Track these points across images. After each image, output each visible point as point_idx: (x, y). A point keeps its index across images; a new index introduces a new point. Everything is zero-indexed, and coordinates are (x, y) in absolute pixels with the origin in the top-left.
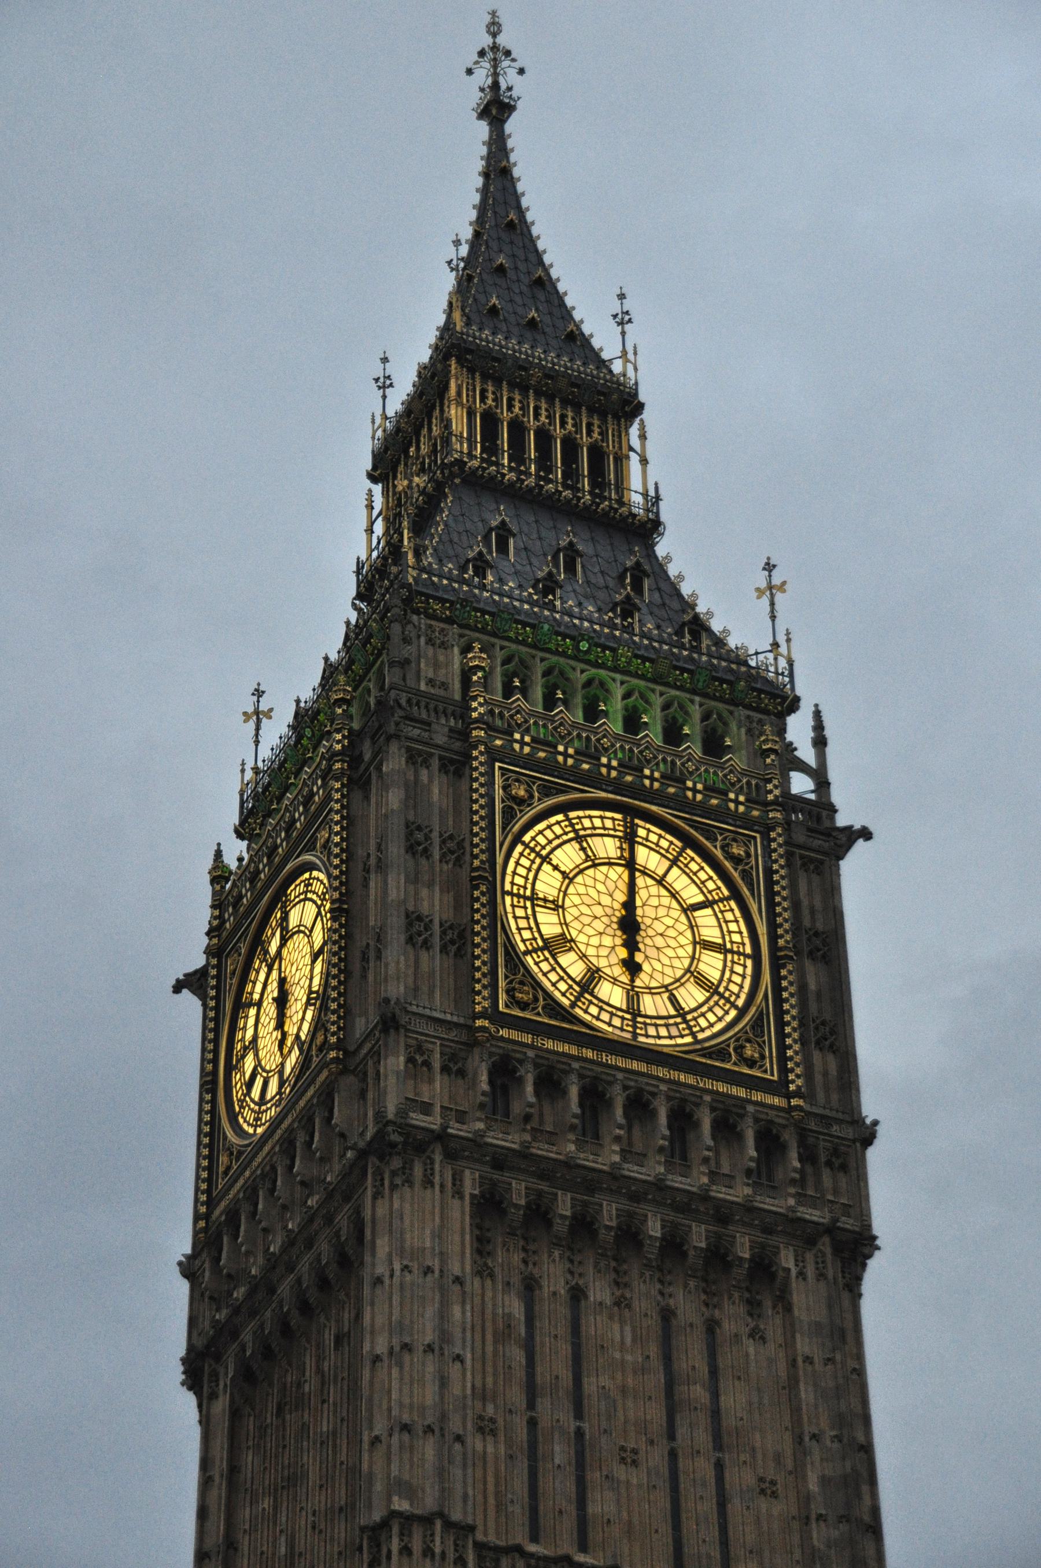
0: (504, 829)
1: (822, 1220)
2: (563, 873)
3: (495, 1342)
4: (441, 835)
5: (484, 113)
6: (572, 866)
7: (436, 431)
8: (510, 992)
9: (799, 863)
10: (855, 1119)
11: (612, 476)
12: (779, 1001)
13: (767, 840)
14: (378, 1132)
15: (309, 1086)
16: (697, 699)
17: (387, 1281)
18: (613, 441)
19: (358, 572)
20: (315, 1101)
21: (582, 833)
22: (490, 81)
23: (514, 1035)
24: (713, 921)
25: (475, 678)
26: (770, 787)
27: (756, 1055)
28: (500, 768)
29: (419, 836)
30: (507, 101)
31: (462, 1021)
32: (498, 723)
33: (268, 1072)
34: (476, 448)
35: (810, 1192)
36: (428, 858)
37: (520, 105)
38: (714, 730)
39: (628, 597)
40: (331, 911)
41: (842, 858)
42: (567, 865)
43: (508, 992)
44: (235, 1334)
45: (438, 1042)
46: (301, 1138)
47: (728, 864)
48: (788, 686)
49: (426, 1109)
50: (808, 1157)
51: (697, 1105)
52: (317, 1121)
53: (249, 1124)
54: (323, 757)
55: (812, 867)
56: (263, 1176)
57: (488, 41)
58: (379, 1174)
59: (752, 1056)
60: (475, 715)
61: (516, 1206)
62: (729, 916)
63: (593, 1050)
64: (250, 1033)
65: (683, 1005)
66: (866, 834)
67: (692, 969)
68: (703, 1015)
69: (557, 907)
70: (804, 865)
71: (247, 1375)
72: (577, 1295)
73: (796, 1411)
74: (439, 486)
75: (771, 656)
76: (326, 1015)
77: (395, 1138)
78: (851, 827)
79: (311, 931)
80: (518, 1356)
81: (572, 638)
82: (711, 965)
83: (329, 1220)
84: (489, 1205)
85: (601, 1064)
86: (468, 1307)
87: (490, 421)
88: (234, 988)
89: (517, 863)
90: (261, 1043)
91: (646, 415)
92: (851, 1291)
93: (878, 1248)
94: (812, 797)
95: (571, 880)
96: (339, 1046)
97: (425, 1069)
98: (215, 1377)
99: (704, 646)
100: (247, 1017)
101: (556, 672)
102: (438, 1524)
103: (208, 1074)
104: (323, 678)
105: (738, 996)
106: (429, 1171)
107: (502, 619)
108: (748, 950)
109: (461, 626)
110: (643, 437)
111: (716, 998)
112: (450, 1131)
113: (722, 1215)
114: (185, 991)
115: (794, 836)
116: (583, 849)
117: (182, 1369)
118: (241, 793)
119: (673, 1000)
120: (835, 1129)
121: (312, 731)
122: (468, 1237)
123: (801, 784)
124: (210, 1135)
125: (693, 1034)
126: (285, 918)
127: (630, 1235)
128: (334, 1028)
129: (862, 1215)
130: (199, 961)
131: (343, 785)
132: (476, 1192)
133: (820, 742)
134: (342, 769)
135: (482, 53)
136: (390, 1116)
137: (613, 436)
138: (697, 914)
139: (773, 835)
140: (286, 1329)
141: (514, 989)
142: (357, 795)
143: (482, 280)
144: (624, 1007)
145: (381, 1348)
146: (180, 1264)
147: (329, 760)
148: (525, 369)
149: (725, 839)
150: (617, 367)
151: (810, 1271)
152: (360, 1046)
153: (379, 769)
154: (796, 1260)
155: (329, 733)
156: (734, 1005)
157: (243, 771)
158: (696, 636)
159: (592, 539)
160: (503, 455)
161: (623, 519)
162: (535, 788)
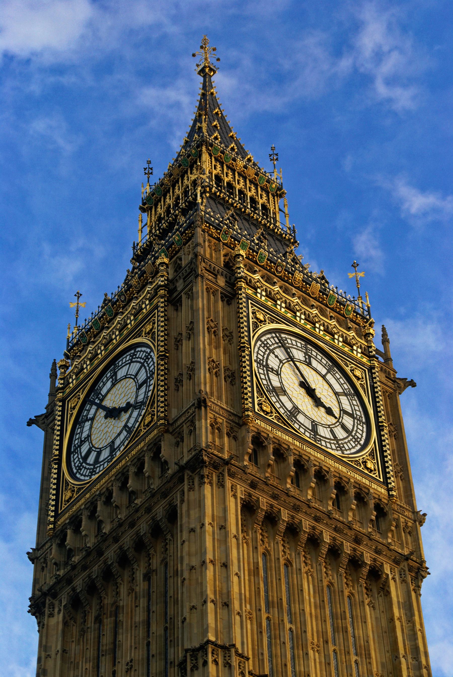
0: (253, 331)
2: (280, 360)
3: (249, 575)
8: (260, 404)
12: (381, 446)
16: (328, 309)
17: (198, 530)
19: (134, 248)
20: (145, 448)
25: (238, 260)
29: (212, 325)
31: (235, 413)
41: (400, 394)
43: (258, 405)
45: (225, 420)
46: (133, 470)
52: (146, 459)
56: (100, 495)
58: (191, 479)
62: (354, 403)
64: (85, 435)
66: (413, 384)
69: (278, 374)
71: (76, 603)
72: (288, 564)
77: (206, 458)
78: (406, 379)
82: (348, 422)
83: (149, 510)
84: (248, 508)
85: (303, 450)
89: (259, 348)
92: (415, 592)
95: (283, 364)
97: (216, 431)
98: (52, 606)
105: (361, 440)
106: (221, 480)
108: (364, 420)
114: (34, 426)
118: (68, 339)
126: (115, 374)
130: (44, 411)
132: (243, 497)
133: (385, 341)
138: (340, 397)
142: (170, 308)
144: (310, 428)
145: (195, 562)
146: (28, 553)
154: (391, 571)
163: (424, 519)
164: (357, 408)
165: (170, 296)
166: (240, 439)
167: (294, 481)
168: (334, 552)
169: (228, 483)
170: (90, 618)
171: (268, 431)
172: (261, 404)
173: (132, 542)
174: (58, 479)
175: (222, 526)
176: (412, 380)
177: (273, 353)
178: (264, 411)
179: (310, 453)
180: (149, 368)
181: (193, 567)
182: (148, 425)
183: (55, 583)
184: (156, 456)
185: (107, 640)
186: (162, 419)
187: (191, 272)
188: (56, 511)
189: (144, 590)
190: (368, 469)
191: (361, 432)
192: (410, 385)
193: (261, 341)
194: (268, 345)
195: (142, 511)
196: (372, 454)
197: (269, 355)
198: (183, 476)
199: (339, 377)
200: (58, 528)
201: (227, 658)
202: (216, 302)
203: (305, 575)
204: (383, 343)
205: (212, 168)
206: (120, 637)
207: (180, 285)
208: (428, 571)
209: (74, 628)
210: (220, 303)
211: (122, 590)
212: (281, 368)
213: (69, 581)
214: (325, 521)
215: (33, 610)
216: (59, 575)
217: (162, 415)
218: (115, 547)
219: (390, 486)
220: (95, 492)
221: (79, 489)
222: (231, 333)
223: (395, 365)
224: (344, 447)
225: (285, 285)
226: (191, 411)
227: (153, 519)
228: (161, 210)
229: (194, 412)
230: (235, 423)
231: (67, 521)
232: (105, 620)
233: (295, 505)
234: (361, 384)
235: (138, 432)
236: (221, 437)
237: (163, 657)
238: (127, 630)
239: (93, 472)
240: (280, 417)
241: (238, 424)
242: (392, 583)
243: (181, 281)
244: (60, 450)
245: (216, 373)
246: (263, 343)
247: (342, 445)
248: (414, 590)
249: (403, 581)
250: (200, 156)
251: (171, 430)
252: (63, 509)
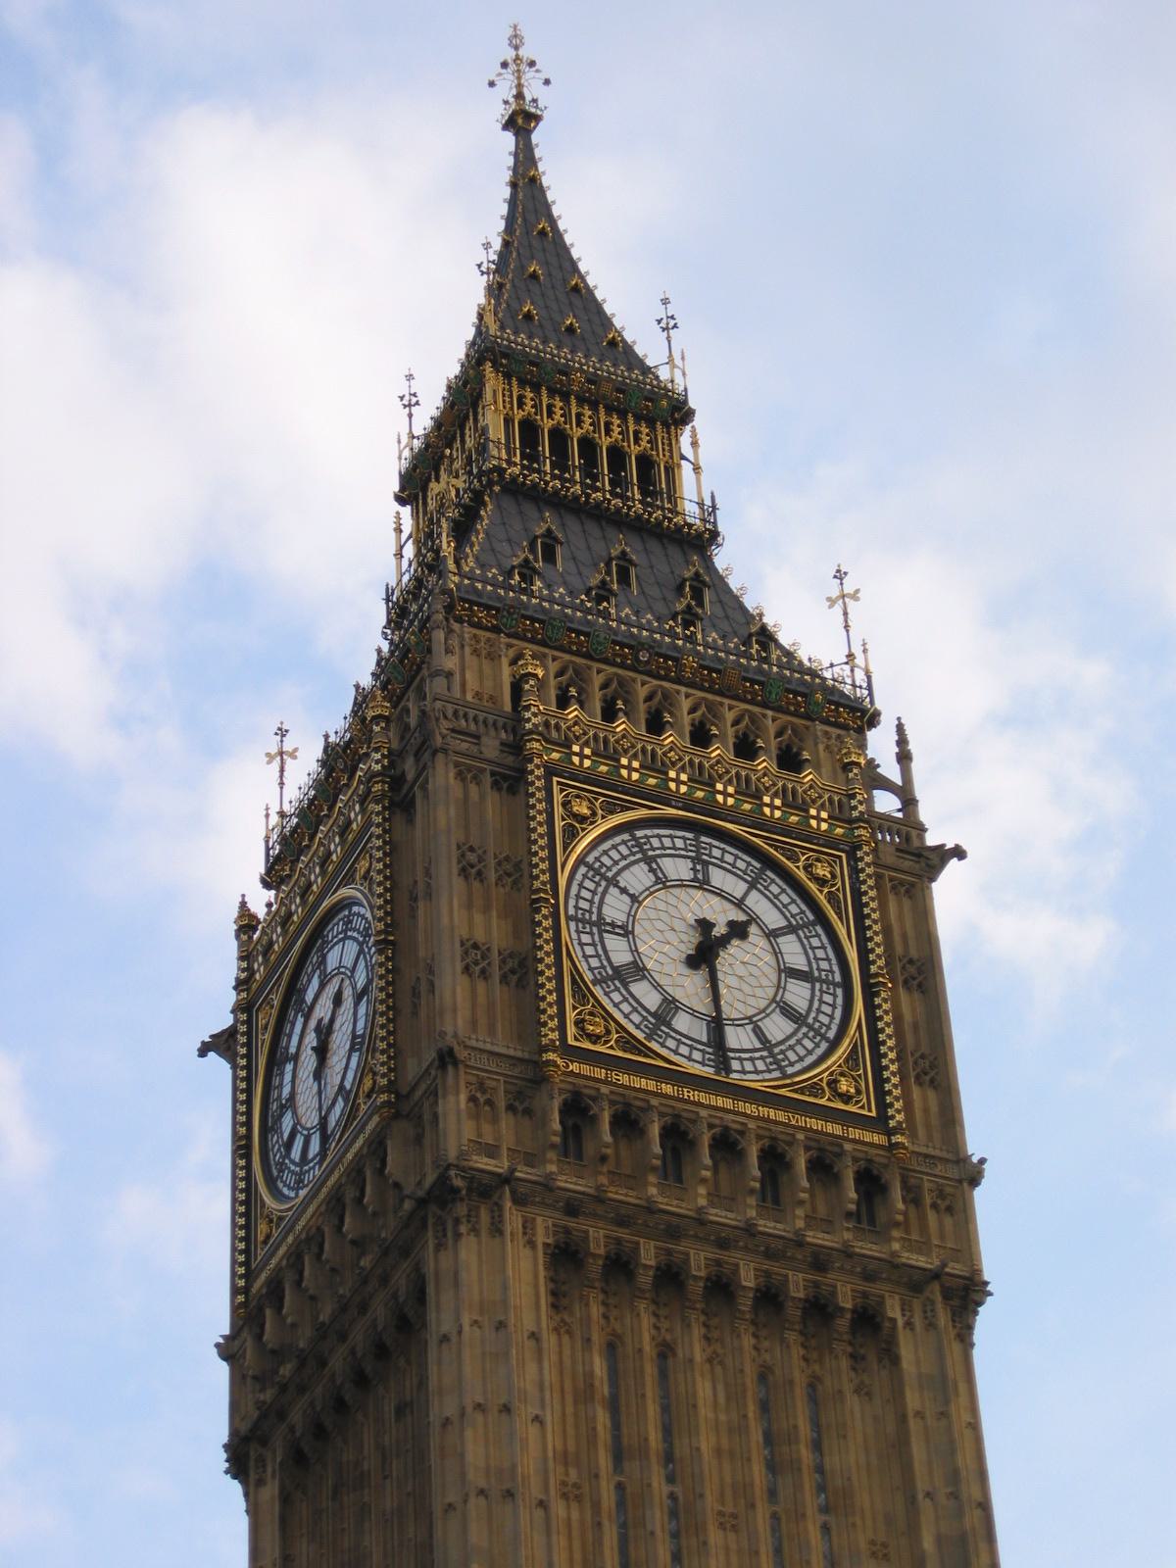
0: (565, 849)
1: (929, 1266)
2: (634, 898)
3: (576, 1402)
4: (496, 857)
5: (510, 124)
6: (641, 888)
7: (470, 443)
9: (889, 885)
10: (960, 1159)
11: (664, 486)
12: (874, 1032)
13: (853, 858)
14: (439, 1178)
15: (356, 1137)
16: (770, 713)
17: (454, 1339)
18: (663, 450)
19: (388, 600)
20: (365, 1151)
21: (650, 853)
22: (514, 92)
23: (586, 1070)
24: (798, 948)
25: (527, 687)
26: (853, 803)
27: (852, 1090)
28: (559, 783)
29: (472, 857)
30: (533, 110)
31: (526, 1056)
32: (554, 734)
33: (308, 1129)
34: (515, 455)
35: (914, 1236)
36: (482, 881)
37: (545, 115)
38: (789, 747)
39: (689, 606)
40: (377, 943)
41: (933, 879)
42: (635, 888)
44: (282, 1415)
46: (350, 1194)
47: (813, 887)
48: (868, 700)
49: (492, 1151)
50: (913, 1197)
51: (790, 1144)
52: (368, 1174)
53: (289, 1188)
54: (360, 782)
55: (903, 890)
56: (308, 1240)
57: (510, 54)
58: (441, 1223)
59: (848, 1091)
60: (528, 726)
61: (594, 1256)
62: (815, 942)
63: (673, 1086)
64: (286, 1091)
65: (770, 1037)
66: (959, 853)
67: (778, 999)
68: (791, 1048)
69: (626, 931)
70: (894, 888)
71: (298, 1458)
74: (478, 498)
75: (847, 668)
76: (373, 1058)
77: (458, 1182)
78: (943, 845)
79: (353, 970)
80: (602, 1418)
81: (630, 647)
82: (798, 994)
83: (385, 1280)
84: (565, 1256)
85: (683, 1100)
86: (546, 1365)
87: (529, 429)
88: (267, 1044)
89: (581, 886)
90: (300, 1100)
91: (698, 421)
93: (990, 1294)
94: (900, 815)
95: (640, 903)
96: (391, 1087)
97: (487, 1108)
98: (261, 1461)
99: (774, 656)
100: (282, 1074)
101: (614, 685)
103: (241, 1138)
104: (355, 704)
105: (829, 1027)
107: (554, 627)
108: (838, 978)
109: (508, 635)
110: (695, 444)
111: (804, 1030)
112: (518, 1174)
113: (819, 1262)
114: (212, 1054)
115: (881, 855)
116: (651, 870)
118: (267, 842)
119: (758, 1032)
120: (939, 1169)
121: (345, 763)
122: (542, 1289)
123: (886, 803)
124: (247, 1203)
125: (781, 1068)
126: (323, 961)
127: (721, 1287)
128: (384, 1069)
129: (972, 1260)
130: (227, 1021)
131: (384, 808)
132: (549, 1241)
133: (904, 757)
134: (383, 790)
135: (504, 65)
137: (663, 444)
138: (778, 940)
139: (859, 854)
140: (340, 1406)
141: (583, 1021)
143: (514, 286)
145: (450, 1410)
146: (217, 1345)
147: (369, 781)
148: (566, 374)
149: (807, 859)
150: (664, 374)
152: (413, 1089)
153: (424, 788)
154: (903, 1310)
155: (367, 755)
156: (824, 1037)
157: (267, 816)
158: (764, 647)
159: (646, 549)
160: (545, 461)
161: (679, 529)
162: (597, 804)
168: (770, 1298)
169: (513, 1219)
175: (500, 1323)
180: (371, 958)
183: (259, 1419)
186: (383, 1093)
193: (587, 865)
194: (603, 870)
196: (853, 1056)
202: (482, 797)
205: (512, 409)
207: (409, 767)
208: (989, 1288)
212: (634, 917)
214: (741, 1244)
216: (264, 1402)
220: (301, 1233)
221: (281, 1219)
223: (924, 814)
224: (787, 1058)
225: (661, 686)
231: (264, 1291)
235: (355, 1108)
239: (299, 1184)
245: (483, 971)
247: (780, 1057)
252: (259, 1258)
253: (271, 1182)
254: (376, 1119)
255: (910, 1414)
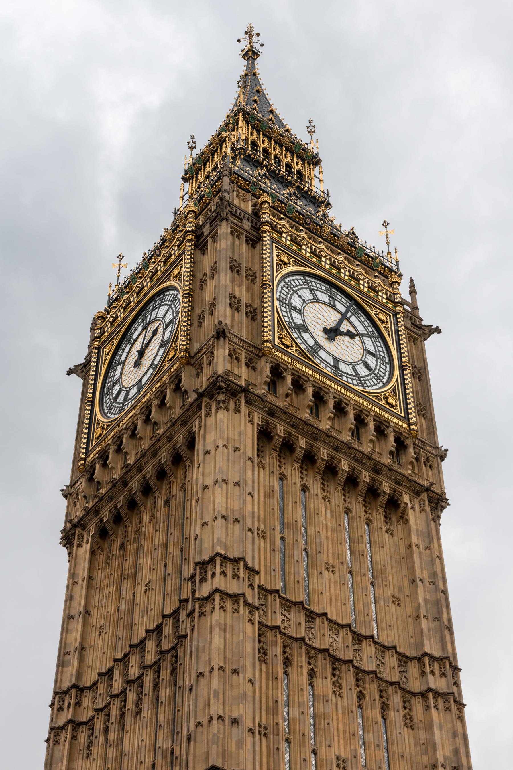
0: (277, 272)
12: (404, 384)
19: (175, 213)
25: (265, 206)
29: (236, 264)
41: (425, 339)
43: (279, 338)
46: (156, 402)
47: (379, 323)
56: (126, 429)
62: (378, 344)
64: (116, 377)
66: (438, 330)
69: (300, 312)
71: (103, 533)
73: (412, 569)
77: (222, 384)
78: (432, 326)
82: (371, 361)
83: (170, 439)
84: (265, 435)
85: (323, 382)
89: (282, 288)
91: (322, 164)
97: (236, 361)
102: (242, 563)
106: (238, 406)
108: (387, 360)
114: (73, 375)
116: (311, 293)
117: (61, 536)
118: (109, 296)
132: (260, 423)
133: (413, 292)
136: (220, 372)
146: (62, 490)
151: (417, 506)
157: (110, 287)
163: (446, 454)
164: (380, 349)
165: (197, 241)
166: (259, 370)
167: (314, 411)
170: (115, 545)
171: (288, 363)
172: (282, 338)
173: (154, 471)
174: (90, 419)
175: (237, 448)
176: (437, 327)
177: (297, 294)
178: (284, 344)
179: (330, 386)
181: (206, 486)
182: (171, 360)
184: (177, 389)
185: (129, 565)
187: (217, 216)
188: (87, 448)
189: (164, 515)
190: (389, 404)
191: (384, 371)
192: (435, 331)
195: (164, 440)
197: (292, 295)
198: (202, 402)
199: (363, 320)
200: (89, 463)
201: (236, 570)
203: (323, 501)
204: (410, 294)
206: (141, 560)
207: (206, 230)
209: (101, 556)
210: (244, 246)
211: (144, 517)
213: (97, 513)
215: (64, 542)
217: (184, 348)
218: (139, 476)
219: (411, 421)
220: (122, 426)
221: (109, 426)
222: (255, 273)
223: (422, 314)
224: (365, 383)
226: (211, 343)
227: (174, 447)
228: (201, 178)
229: (213, 343)
230: (255, 354)
232: (129, 547)
233: (313, 433)
234: (385, 327)
235: (162, 366)
236: (239, 367)
237: (178, 575)
238: (147, 554)
240: (300, 351)
241: (258, 356)
242: (410, 512)
243: (208, 225)
244: (94, 393)
245: (237, 309)
246: (287, 283)
248: (433, 519)
249: (423, 510)
250: (237, 124)
251: (192, 362)
253: (104, 414)
254: (177, 364)
255: (414, 545)
